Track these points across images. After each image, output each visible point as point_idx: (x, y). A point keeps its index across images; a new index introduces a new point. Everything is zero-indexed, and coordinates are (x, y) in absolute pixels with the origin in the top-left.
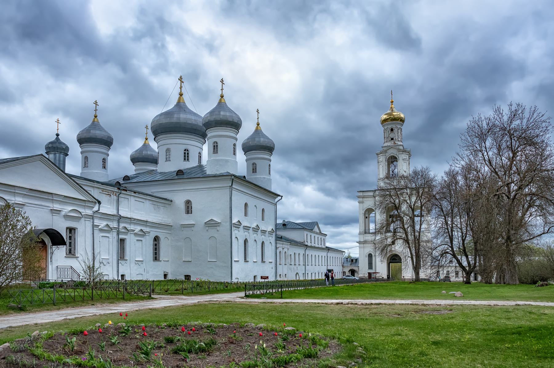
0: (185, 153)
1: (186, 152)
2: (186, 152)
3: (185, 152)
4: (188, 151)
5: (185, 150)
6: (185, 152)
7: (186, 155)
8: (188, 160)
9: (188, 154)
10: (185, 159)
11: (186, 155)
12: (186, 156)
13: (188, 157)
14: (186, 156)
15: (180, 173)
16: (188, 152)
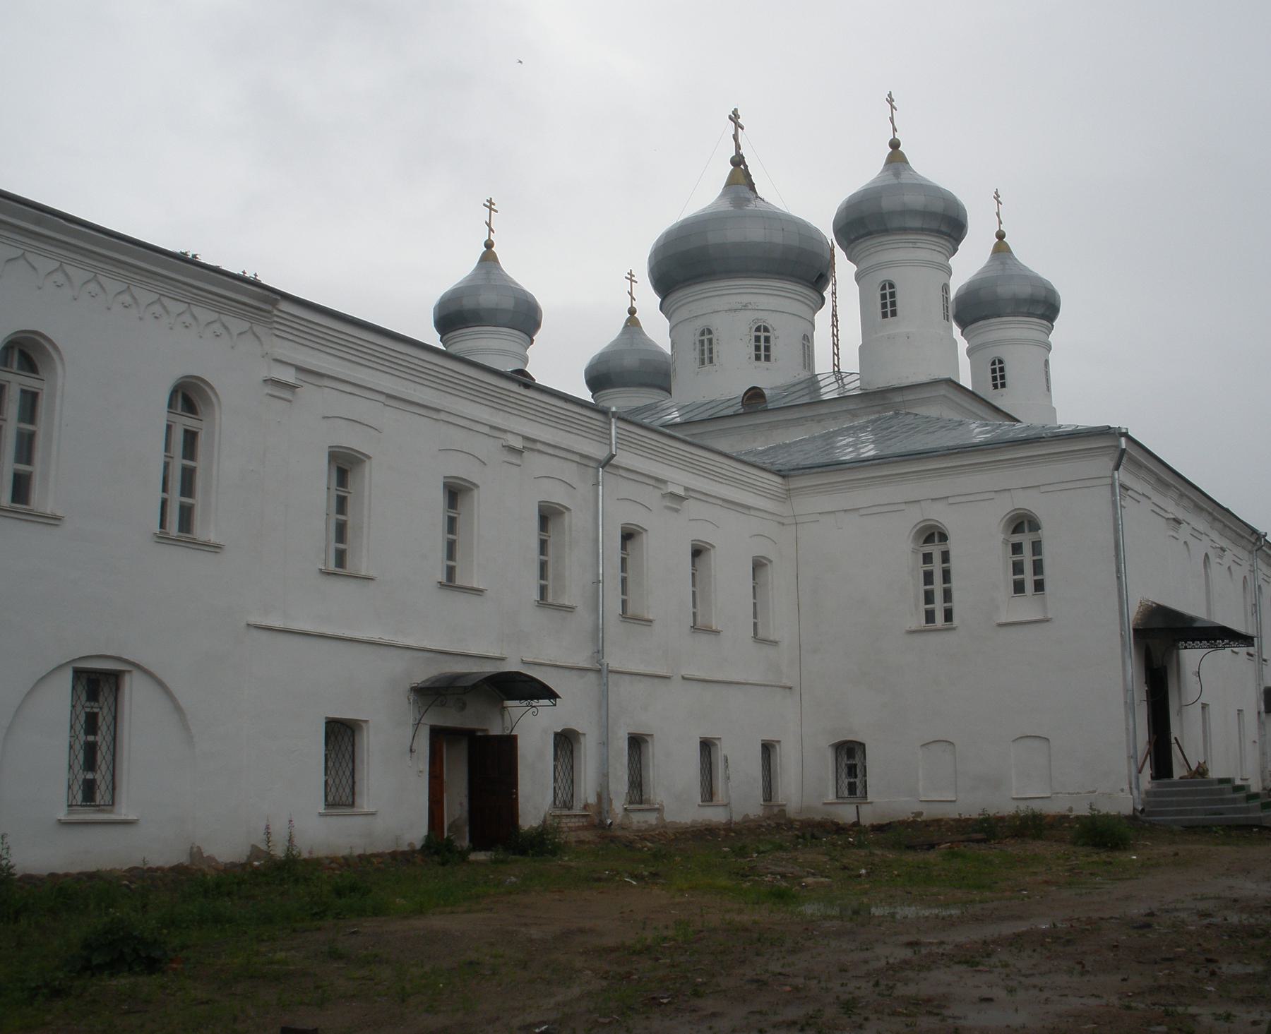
0: (757, 339)
1: (762, 334)
2: (762, 334)
3: (758, 334)
4: (766, 330)
5: (758, 329)
6: (758, 334)
7: (762, 344)
8: (767, 358)
9: (767, 339)
10: (758, 358)
11: (762, 344)
12: (762, 348)
13: (767, 349)
14: (762, 348)
15: (754, 397)
16: (766, 334)
